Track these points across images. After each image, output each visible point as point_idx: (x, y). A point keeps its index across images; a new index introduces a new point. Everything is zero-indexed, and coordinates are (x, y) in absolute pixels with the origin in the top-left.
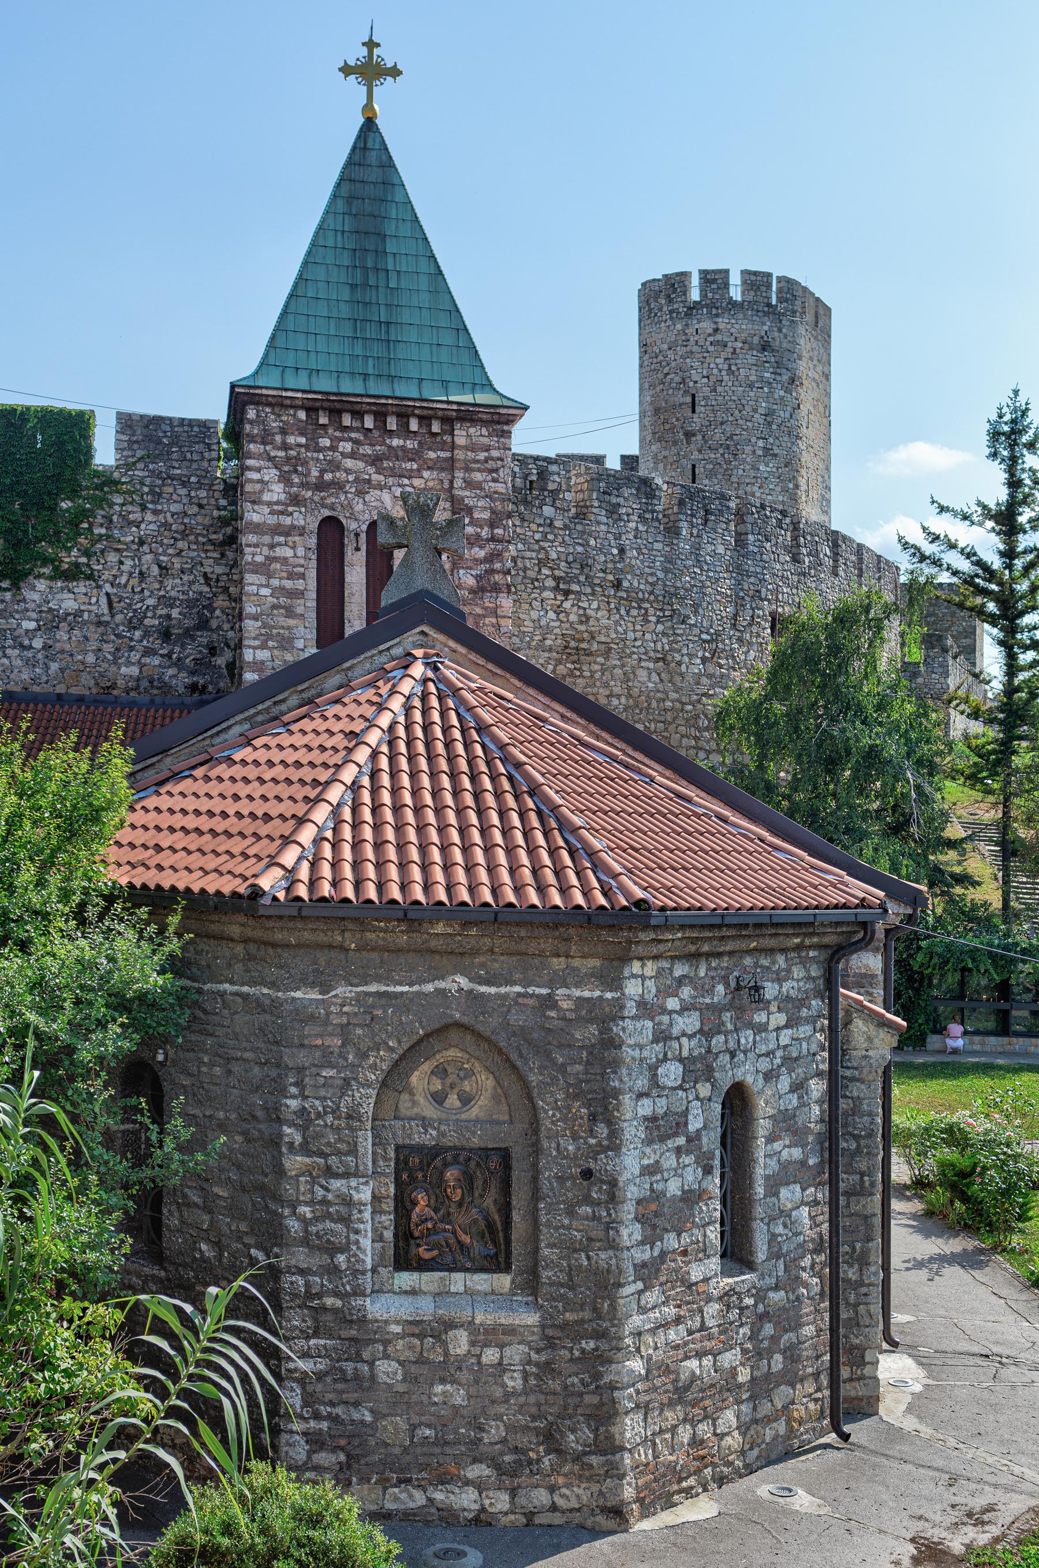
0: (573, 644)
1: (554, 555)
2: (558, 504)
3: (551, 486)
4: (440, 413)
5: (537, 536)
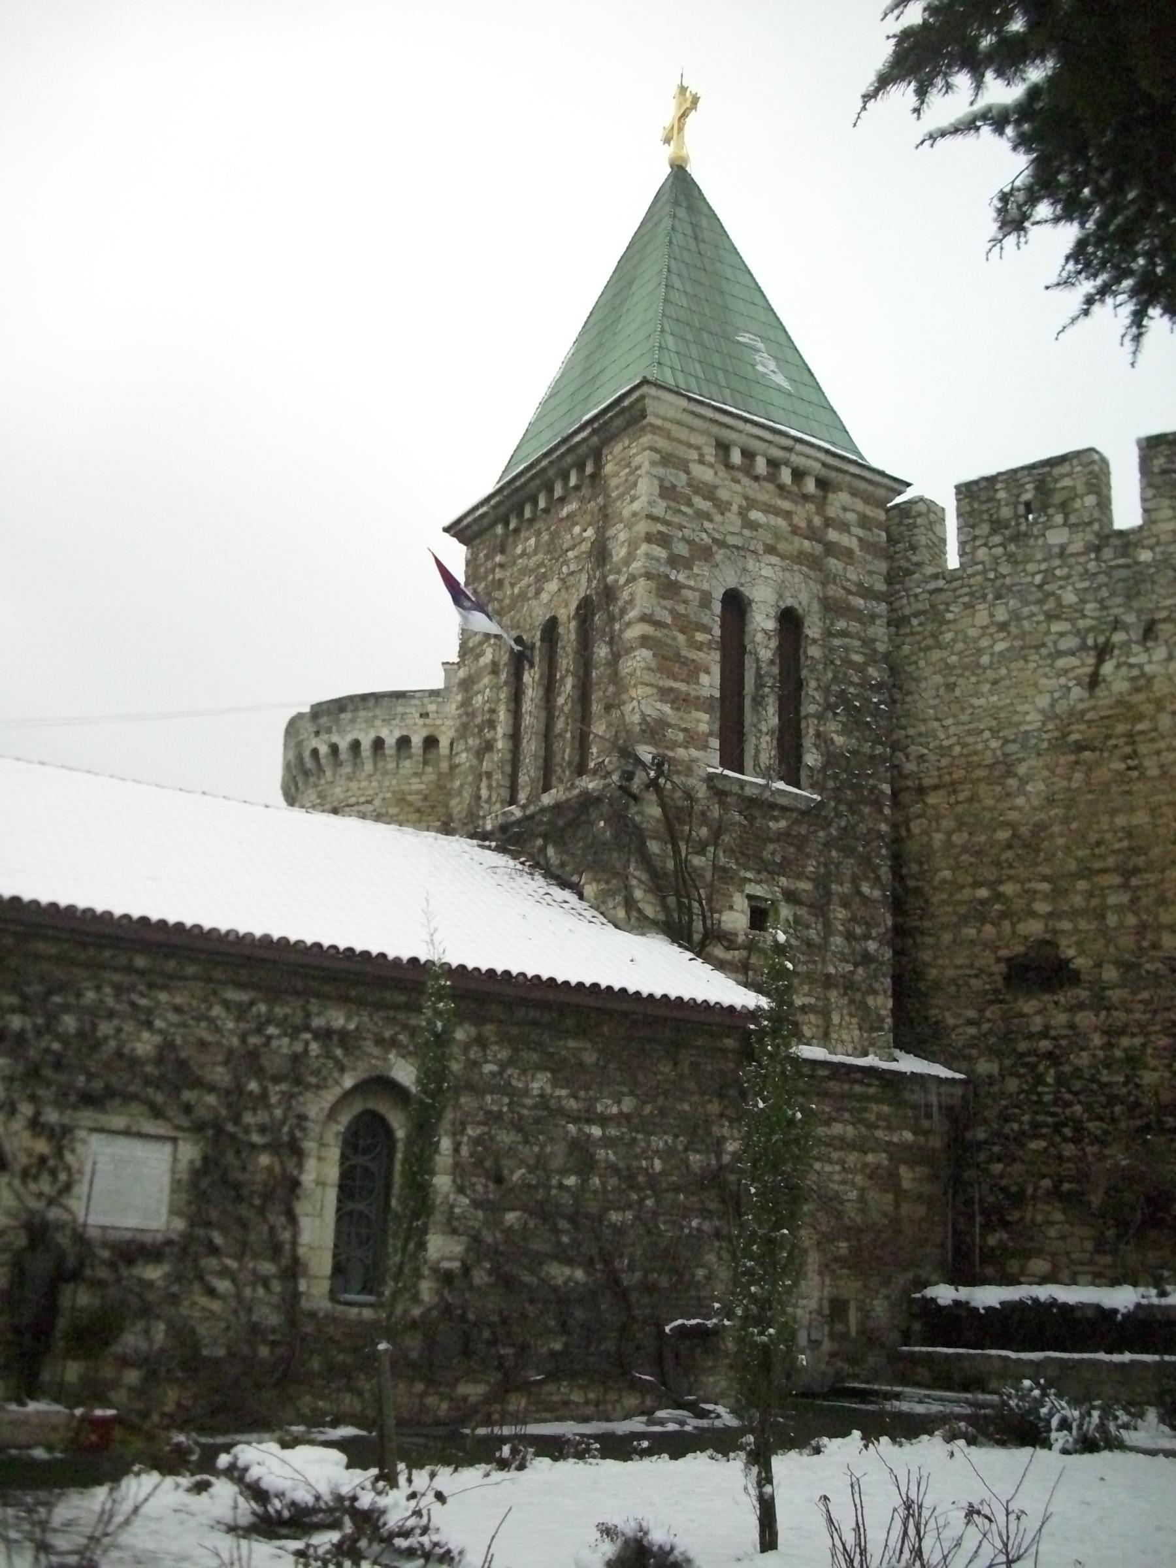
0: (1121, 728)
1: (1069, 597)
2: (1073, 519)
3: (1057, 498)
4: (583, 449)
5: (1038, 579)
